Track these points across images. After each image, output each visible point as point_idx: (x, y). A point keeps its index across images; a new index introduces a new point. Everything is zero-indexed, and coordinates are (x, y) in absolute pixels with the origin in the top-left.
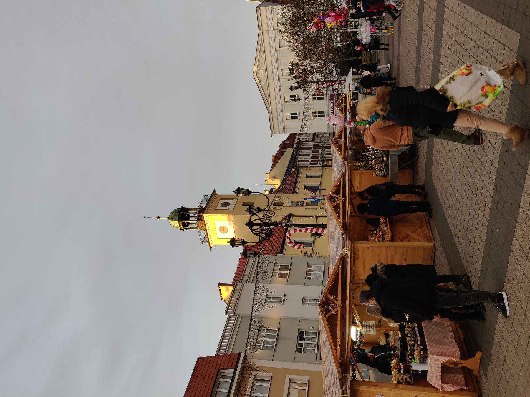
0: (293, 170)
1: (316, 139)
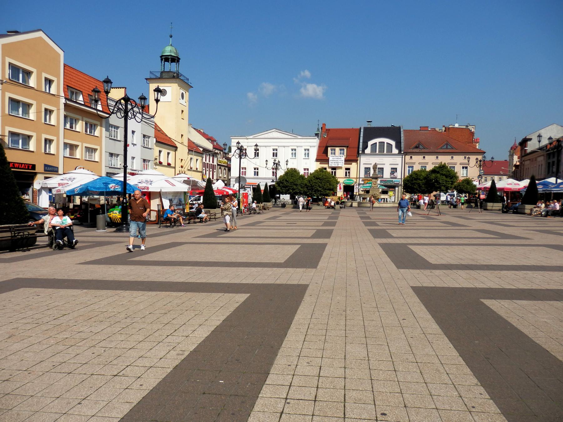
1: (219, 167)
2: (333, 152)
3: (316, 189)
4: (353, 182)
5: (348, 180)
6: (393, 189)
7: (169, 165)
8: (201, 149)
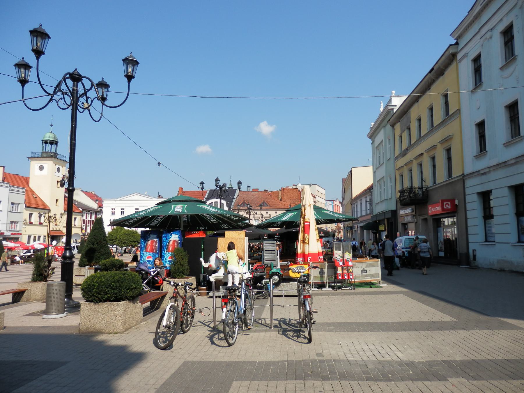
0: (81, 209)
3: (123, 241)
7: (41, 224)
8: (81, 209)
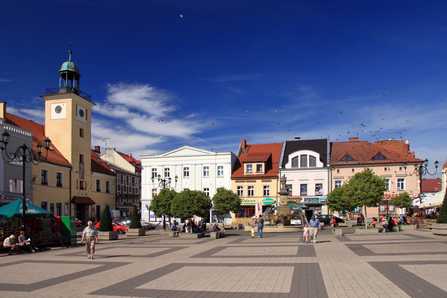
2: (250, 168)
4: (273, 201)
5: (267, 199)
6: (319, 208)
